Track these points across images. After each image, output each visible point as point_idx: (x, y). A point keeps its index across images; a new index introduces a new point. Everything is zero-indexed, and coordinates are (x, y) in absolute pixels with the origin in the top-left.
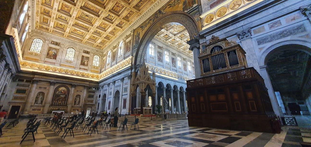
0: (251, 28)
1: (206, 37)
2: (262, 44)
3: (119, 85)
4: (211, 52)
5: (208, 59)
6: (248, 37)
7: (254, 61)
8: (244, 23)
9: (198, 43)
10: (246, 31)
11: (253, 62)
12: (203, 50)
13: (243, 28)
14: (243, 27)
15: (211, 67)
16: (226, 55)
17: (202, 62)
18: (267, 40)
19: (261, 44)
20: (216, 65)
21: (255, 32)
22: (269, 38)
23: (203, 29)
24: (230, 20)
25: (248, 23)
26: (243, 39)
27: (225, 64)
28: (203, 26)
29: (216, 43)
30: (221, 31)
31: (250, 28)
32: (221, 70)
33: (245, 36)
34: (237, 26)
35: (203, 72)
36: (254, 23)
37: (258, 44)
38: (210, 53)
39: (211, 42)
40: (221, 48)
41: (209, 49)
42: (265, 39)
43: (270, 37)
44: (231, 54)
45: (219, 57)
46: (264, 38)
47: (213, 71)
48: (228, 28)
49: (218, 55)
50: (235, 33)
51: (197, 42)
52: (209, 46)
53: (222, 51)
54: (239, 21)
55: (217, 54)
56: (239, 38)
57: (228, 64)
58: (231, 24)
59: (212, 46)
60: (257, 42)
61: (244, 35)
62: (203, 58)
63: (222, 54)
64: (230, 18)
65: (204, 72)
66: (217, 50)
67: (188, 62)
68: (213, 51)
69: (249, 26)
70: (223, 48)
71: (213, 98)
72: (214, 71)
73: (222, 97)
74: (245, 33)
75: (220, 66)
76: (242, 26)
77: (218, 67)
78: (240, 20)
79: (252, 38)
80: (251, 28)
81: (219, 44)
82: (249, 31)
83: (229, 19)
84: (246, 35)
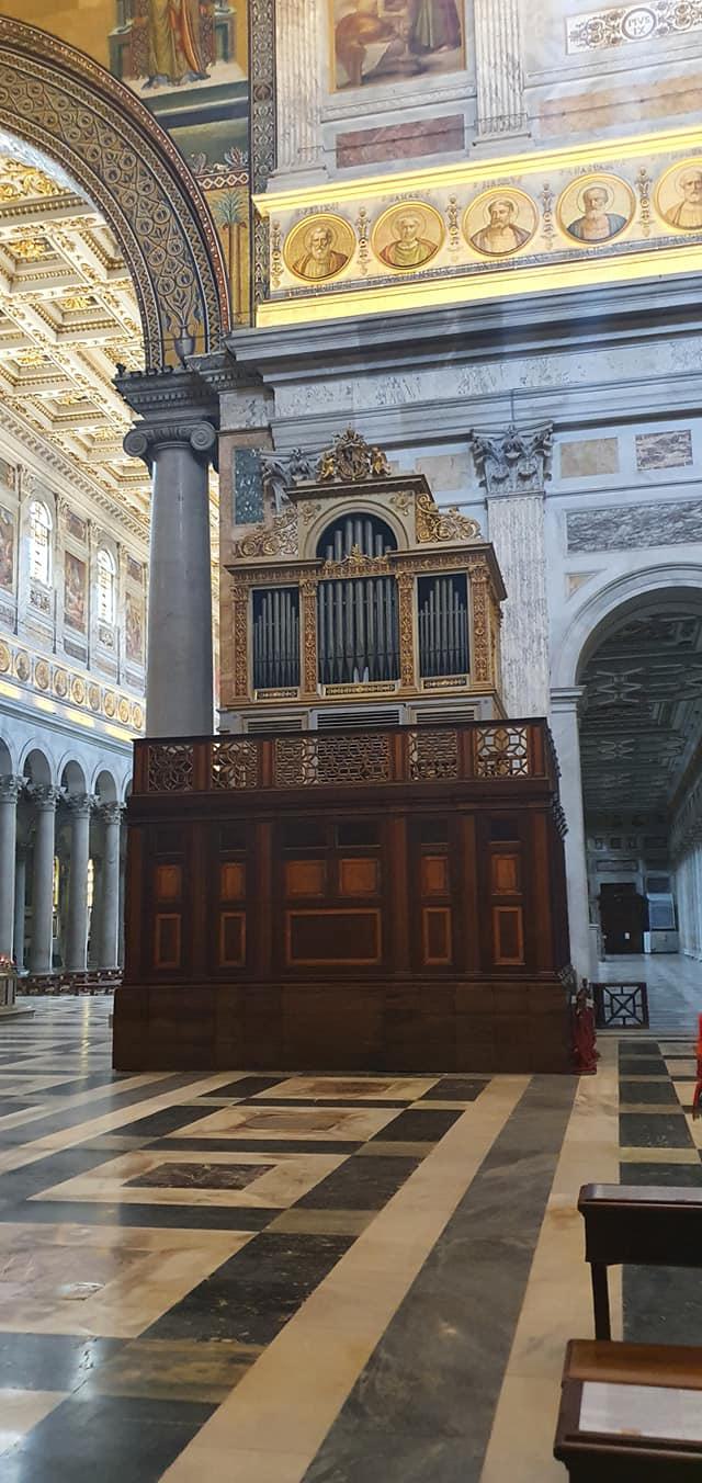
0: (558, 428)
1: (277, 390)
2: (590, 551)
4: (321, 551)
5: (294, 593)
6: (528, 482)
7: (530, 648)
8: (523, 380)
9: (202, 412)
10: (527, 442)
11: (525, 651)
12: (238, 484)
14: (519, 404)
15: (308, 663)
16: (408, 594)
17: (250, 605)
18: (614, 537)
20: (340, 653)
21: (571, 468)
23: (270, 317)
24: (451, 321)
25: (545, 384)
26: (501, 488)
27: (396, 655)
28: (260, 292)
30: (381, 380)
32: (362, 694)
33: (514, 472)
35: (250, 683)
36: (574, 397)
37: (570, 547)
38: (311, 554)
39: (330, 477)
40: (390, 540)
41: (312, 521)
42: (604, 525)
46: (605, 514)
47: (319, 691)
48: (431, 376)
50: (467, 431)
51: (200, 405)
52: (315, 502)
53: (393, 562)
55: (357, 575)
56: (481, 469)
58: (450, 356)
59: (333, 509)
61: (511, 462)
62: (263, 581)
63: (389, 583)
66: (359, 545)
67: (101, 554)
69: (543, 413)
71: (304, 877)
72: (321, 690)
73: (358, 876)
74: (517, 447)
75: (361, 661)
76: (513, 395)
77: (350, 661)
78: (508, 349)
79: (545, 496)
80: (558, 428)
81: (379, 504)
82: (541, 447)
83: (449, 314)
84: (521, 467)
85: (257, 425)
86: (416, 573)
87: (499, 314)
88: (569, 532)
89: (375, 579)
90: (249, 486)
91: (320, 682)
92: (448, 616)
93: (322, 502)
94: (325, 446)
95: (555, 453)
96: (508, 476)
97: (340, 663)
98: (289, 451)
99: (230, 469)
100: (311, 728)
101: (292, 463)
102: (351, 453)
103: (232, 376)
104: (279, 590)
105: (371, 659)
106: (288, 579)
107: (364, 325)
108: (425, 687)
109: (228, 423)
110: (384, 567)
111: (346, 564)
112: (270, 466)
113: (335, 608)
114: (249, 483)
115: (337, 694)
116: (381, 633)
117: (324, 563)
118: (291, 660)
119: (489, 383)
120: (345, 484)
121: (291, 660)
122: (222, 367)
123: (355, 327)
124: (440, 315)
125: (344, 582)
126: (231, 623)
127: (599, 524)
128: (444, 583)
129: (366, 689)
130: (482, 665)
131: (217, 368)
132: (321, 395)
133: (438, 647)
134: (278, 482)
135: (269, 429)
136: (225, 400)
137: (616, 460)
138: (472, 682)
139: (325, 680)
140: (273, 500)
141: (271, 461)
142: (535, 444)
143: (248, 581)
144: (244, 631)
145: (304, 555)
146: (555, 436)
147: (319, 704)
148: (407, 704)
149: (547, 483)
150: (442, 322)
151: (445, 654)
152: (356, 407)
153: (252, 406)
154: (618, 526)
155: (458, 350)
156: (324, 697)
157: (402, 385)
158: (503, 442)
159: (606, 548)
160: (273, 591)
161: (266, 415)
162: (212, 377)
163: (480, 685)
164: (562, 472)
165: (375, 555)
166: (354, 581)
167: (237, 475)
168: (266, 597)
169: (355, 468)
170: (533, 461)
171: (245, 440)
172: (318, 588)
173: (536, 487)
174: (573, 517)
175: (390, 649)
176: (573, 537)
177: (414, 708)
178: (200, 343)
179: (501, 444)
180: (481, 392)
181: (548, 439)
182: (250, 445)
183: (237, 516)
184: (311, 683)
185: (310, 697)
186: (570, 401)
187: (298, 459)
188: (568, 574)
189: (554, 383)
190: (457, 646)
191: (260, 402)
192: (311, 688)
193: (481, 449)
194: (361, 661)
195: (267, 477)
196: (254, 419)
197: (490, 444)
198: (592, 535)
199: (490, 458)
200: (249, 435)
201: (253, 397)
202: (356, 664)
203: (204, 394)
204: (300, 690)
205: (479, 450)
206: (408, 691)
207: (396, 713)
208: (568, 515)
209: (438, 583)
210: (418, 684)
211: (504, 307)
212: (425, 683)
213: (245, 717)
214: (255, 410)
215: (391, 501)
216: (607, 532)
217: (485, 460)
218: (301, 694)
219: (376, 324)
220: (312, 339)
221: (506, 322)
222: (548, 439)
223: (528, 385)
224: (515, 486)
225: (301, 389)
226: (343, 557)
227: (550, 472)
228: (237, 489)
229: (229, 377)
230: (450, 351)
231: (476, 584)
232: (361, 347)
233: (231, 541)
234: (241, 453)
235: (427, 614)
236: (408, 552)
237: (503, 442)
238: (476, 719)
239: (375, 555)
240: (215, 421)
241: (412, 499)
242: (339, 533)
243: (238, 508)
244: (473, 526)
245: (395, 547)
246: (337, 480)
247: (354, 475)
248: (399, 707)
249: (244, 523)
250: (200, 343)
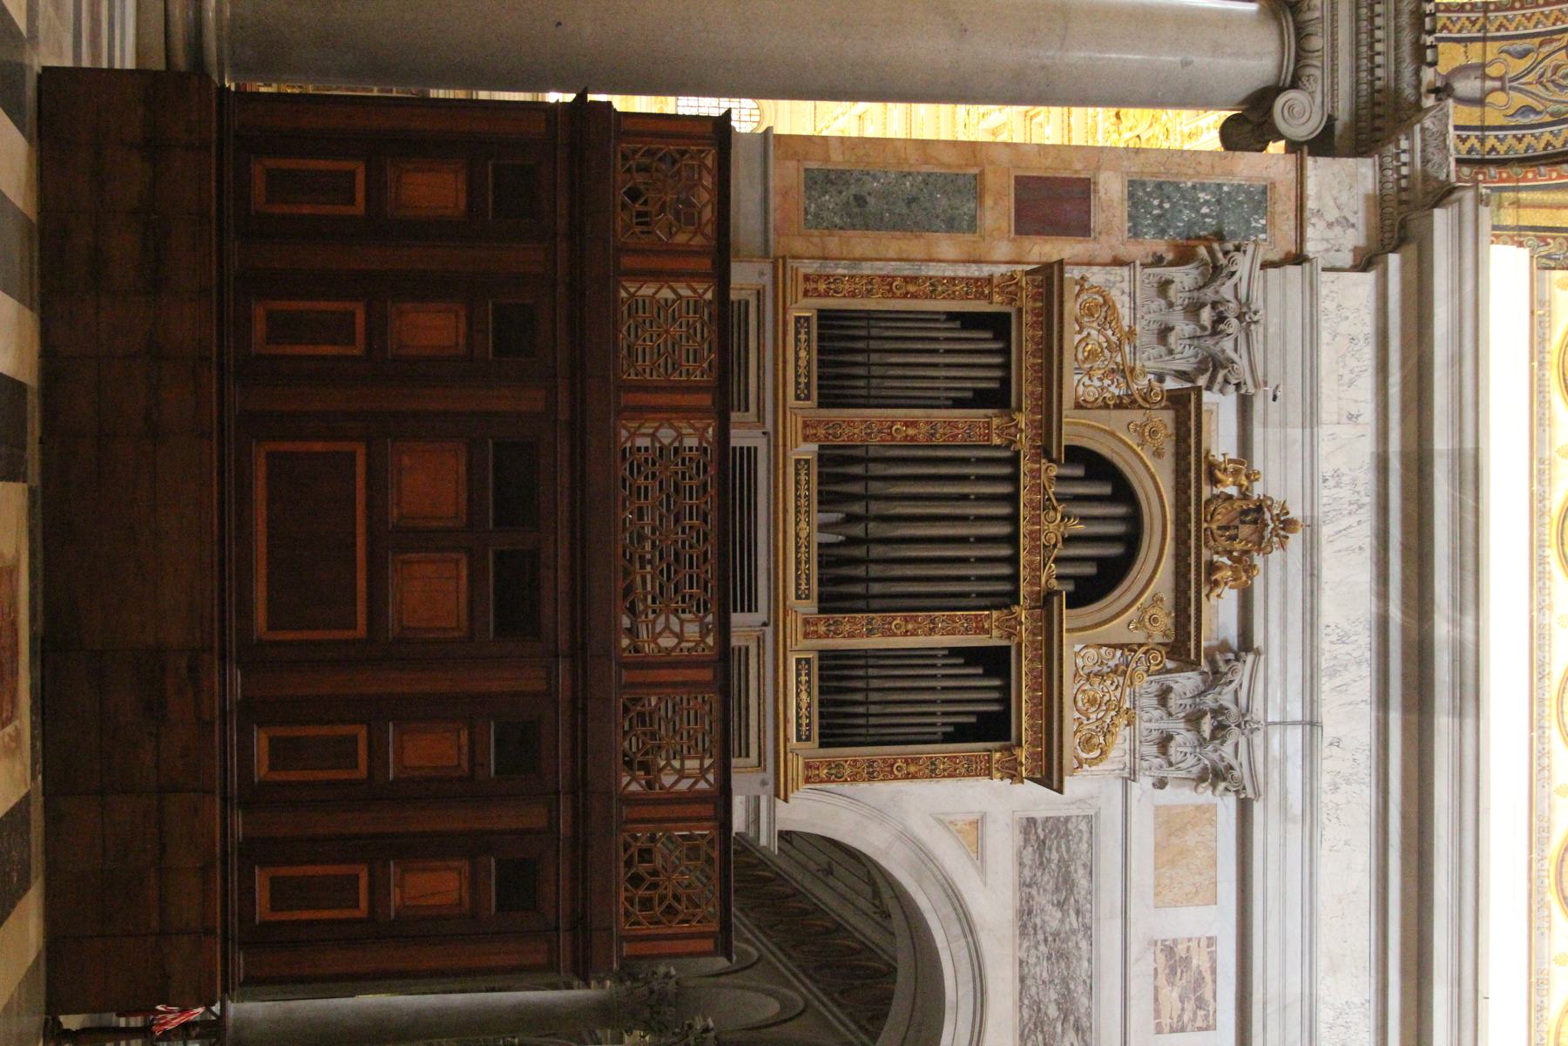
0: (1244, 811)
1: (1369, 278)
2: (1020, 855)
4: (1076, 454)
5: (997, 398)
6: (1154, 749)
8: (1336, 743)
9: (1343, 115)
10: (1227, 750)
12: (1204, 188)
13: (1283, 723)
14: (1295, 736)
16: (982, 630)
18: (1042, 900)
19: (1026, 840)
21: (1170, 825)
22: (1062, 921)
24: (1457, 623)
29: (1181, 541)
30: (1366, 479)
31: (1250, 793)
34: (1334, 673)
36: (1295, 832)
37: (1031, 822)
38: (1076, 430)
39: (1215, 481)
40: (1087, 591)
42: (1066, 882)
43: (1074, 932)
45: (981, 540)
48: (1362, 574)
49: (1013, 540)
50: (1258, 641)
51: (1356, 116)
52: (1169, 448)
53: (1045, 600)
54: (1383, 702)
57: (851, 635)
60: (1063, 813)
61: (1194, 720)
62: (1025, 336)
64: (1469, 636)
65: (824, 315)
66: (1080, 528)
68: (1088, 477)
69: (1274, 776)
70: (1070, 618)
72: (809, 450)
74: (1220, 730)
75: (858, 530)
76: (1312, 724)
77: (858, 508)
78: (1395, 718)
79: (1131, 776)
80: (1244, 811)
82: (1215, 775)
83: (1469, 621)
84: (1184, 739)
85: (1310, 232)
86: (1019, 645)
87: (1459, 712)
88: (1058, 819)
89: (1014, 560)
90: (1198, 211)
91: (821, 447)
92: (933, 702)
93: (1168, 462)
94: (1260, 373)
95: (1205, 795)
96: (1170, 715)
97: (857, 488)
98: (1257, 303)
99: (1232, 174)
100: (733, 432)
101: (1233, 305)
102: (1255, 522)
103: (1405, 189)
104: (1006, 366)
105: (858, 552)
106: (1027, 388)
107: (1469, 463)
108: (798, 661)
109: (1319, 171)
110: (1035, 580)
111: (1047, 506)
112: (1232, 262)
113: (964, 478)
114: (1205, 210)
115: (797, 482)
116: (910, 571)
117: (1051, 460)
118: (868, 387)
119: (1337, 681)
120: (1198, 512)
121: (868, 387)
122: (1424, 172)
123: (1469, 444)
124: (1470, 605)
125: (1013, 499)
126: (942, 164)
127: (1068, 873)
128: (995, 695)
129: (802, 541)
130: (836, 775)
131: (1425, 161)
132: (1352, 362)
133: (875, 683)
134: (1202, 274)
135: (1298, 258)
136: (1363, 170)
137: (1175, 904)
138: (801, 752)
139: (828, 457)
140: (1170, 256)
141: (1243, 264)
142: (1221, 766)
143: (1028, 305)
144: (932, 295)
145: (1068, 423)
146: (1231, 801)
147: (775, 441)
148: (769, 630)
149: (1150, 781)
150: (1459, 606)
151: (859, 697)
152: (1324, 432)
153: (1346, 223)
154: (1060, 905)
155: (1405, 629)
156: (792, 457)
157: (1352, 520)
158: (1232, 707)
159: (1024, 885)
160: (1006, 352)
161: (1327, 250)
162: (1409, 148)
163: (797, 766)
164: (1168, 808)
165: (1058, 560)
166: (1014, 519)
167: (1220, 186)
168: (995, 339)
169: (1226, 528)
170: (1191, 760)
171: (1284, 207)
172: (1007, 447)
173: (1145, 764)
174: (1083, 826)
175: (876, 588)
176: (1049, 824)
177: (760, 641)
178: (1470, 115)
179: (1226, 699)
180: (1324, 665)
181: (1227, 789)
182: (1273, 214)
183: (1143, 184)
184: (821, 432)
185: (795, 424)
186: (1290, 826)
187: (1240, 317)
188: (983, 817)
189: (1326, 798)
190: (874, 709)
191: (1355, 238)
192: (811, 431)
193: (1223, 668)
194: (858, 530)
195: (1211, 252)
196: (1321, 225)
197: (1231, 682)
198: (1049, 861)
199: (1204, 682)
200: (1292, 216)
201: (1361, 227)
202: (851, 519)
203: (1378, 123)
204: (810, 408)
205: (1221, 663)
206: (795, 626)
207: (752, 607)
208: (1089, 819)
209: (997, 683)
211: (1469, 723)
212: (808, 661)
213: (759, 294)
214: (1337, 230)
215: (1156, 600)
216: (1051, 886)
217: (1203, 673)
218: (802, 411)
219: (1469, 488)
220: (1457, 359)
221: (1443, 723)
222: (1227, 789)
223: (1326, 752)
224: (1148, 725)
225: (1365, 325)
226: (1061, 499)
227: (1168, 787)
228: (1194, 187)
229: (1403, 183)
230: (1404, 613)
231: (989, 760)
232: (1431, 450)
233: (1098, 168)
234: (1260, 198)
235: (940, 662)
236: (1061, 631)
237: (1232, 707)
238: (734, 761)
239: (1058, 560)
240: (1323, 144)
241: (1158, 638)
242: (1106, 490)
243: (1159, 186)
244: (1096, 753)
245: (1076, 601)
246: (1207, 491)
247: (1214, 526)
248: (761, 615)
249: (1131, 195)
250: (1470, 115)
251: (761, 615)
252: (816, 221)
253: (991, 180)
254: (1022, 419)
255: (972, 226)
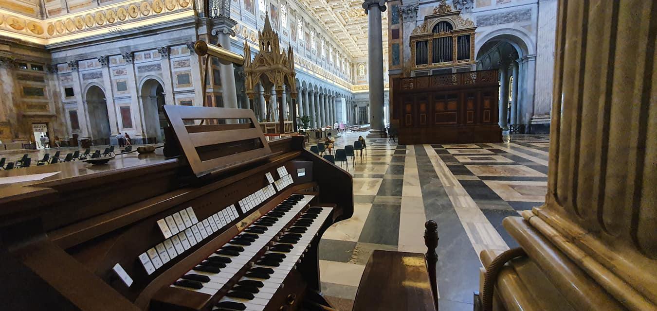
3: (153, 66)
5: (426, 42)
15: (429, 58)
16: (455, 40)
17: (415, 45)
32: (443, 65)
44: (461, 41)
71: (440, 106)
72: (433, 64)
73: (452, 105)
75: (442, 57)
77: (440, 57)
105: (445, 57)
147: (432, 68)
185: (430, 66)
194: (442, 57)
202: (441, 58)
206: (454, 64)
210: (457, 62)
251: (453, 68)
252: (399, 64)
253: (393, 43)
254: (429, 39)
255: (398, 44)
